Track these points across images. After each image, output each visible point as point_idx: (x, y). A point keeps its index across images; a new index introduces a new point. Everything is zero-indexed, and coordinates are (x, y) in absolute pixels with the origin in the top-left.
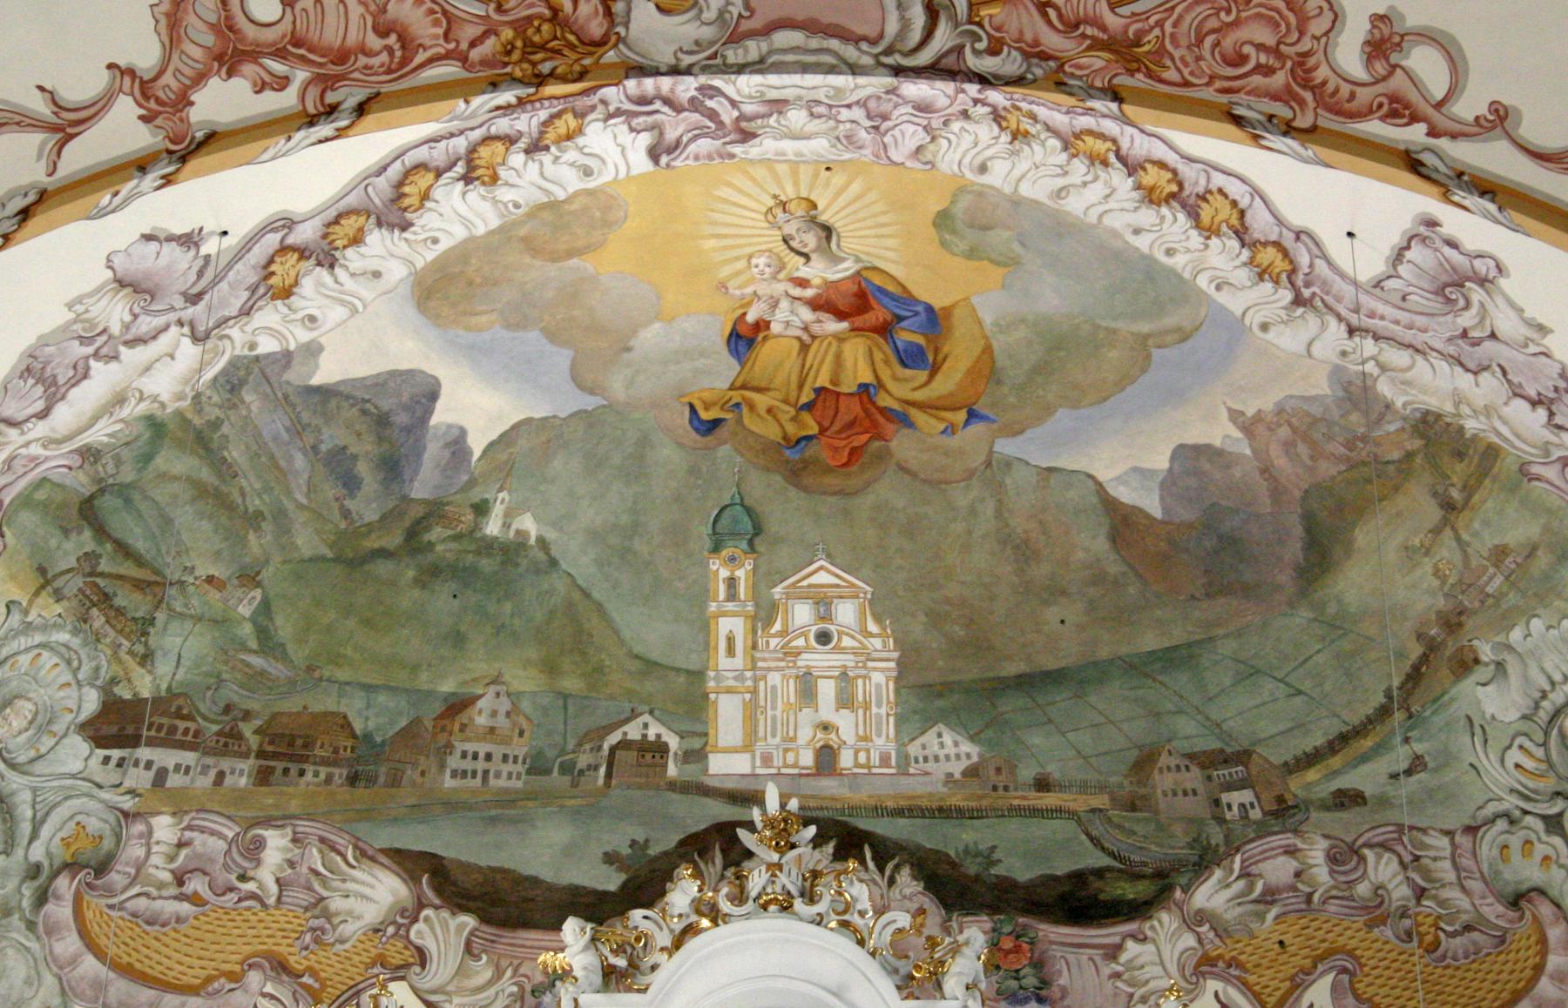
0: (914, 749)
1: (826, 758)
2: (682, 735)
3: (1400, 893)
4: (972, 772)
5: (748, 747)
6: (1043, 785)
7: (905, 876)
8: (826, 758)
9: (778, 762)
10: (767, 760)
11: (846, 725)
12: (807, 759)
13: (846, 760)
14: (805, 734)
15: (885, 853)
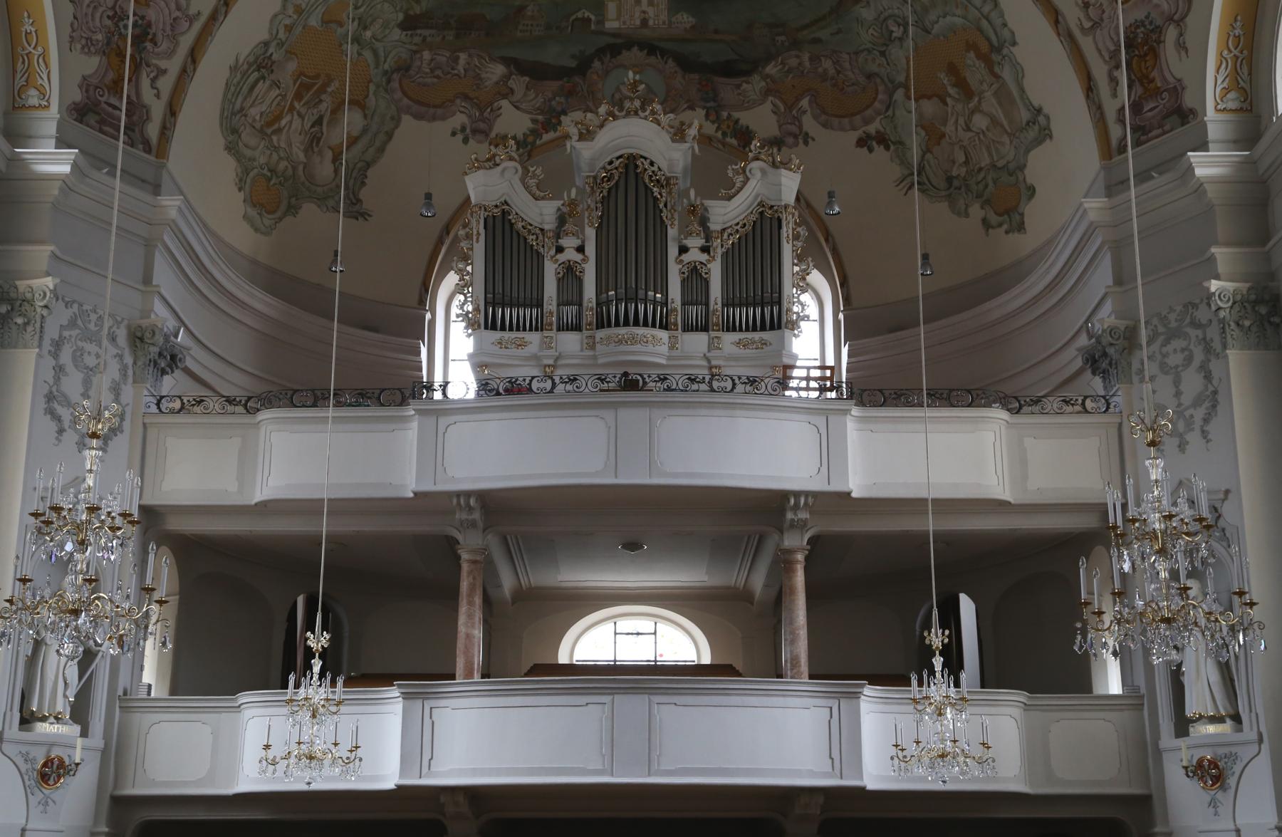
0: (673, 20)
1: (644, 22)
2: (595, 15)
3: (832, 72)
4: (693, 27)
5: (618, 19)
6: (716, 32)
7: (670, 61)
8: (644, 22)
9: (628, 23)
10: (624, 23)
11: (651, 12)
12: (638, 22)
13: (651, 23)
14: (637, 14)
15: (664, 53)
